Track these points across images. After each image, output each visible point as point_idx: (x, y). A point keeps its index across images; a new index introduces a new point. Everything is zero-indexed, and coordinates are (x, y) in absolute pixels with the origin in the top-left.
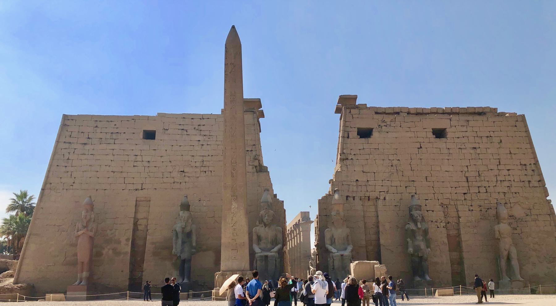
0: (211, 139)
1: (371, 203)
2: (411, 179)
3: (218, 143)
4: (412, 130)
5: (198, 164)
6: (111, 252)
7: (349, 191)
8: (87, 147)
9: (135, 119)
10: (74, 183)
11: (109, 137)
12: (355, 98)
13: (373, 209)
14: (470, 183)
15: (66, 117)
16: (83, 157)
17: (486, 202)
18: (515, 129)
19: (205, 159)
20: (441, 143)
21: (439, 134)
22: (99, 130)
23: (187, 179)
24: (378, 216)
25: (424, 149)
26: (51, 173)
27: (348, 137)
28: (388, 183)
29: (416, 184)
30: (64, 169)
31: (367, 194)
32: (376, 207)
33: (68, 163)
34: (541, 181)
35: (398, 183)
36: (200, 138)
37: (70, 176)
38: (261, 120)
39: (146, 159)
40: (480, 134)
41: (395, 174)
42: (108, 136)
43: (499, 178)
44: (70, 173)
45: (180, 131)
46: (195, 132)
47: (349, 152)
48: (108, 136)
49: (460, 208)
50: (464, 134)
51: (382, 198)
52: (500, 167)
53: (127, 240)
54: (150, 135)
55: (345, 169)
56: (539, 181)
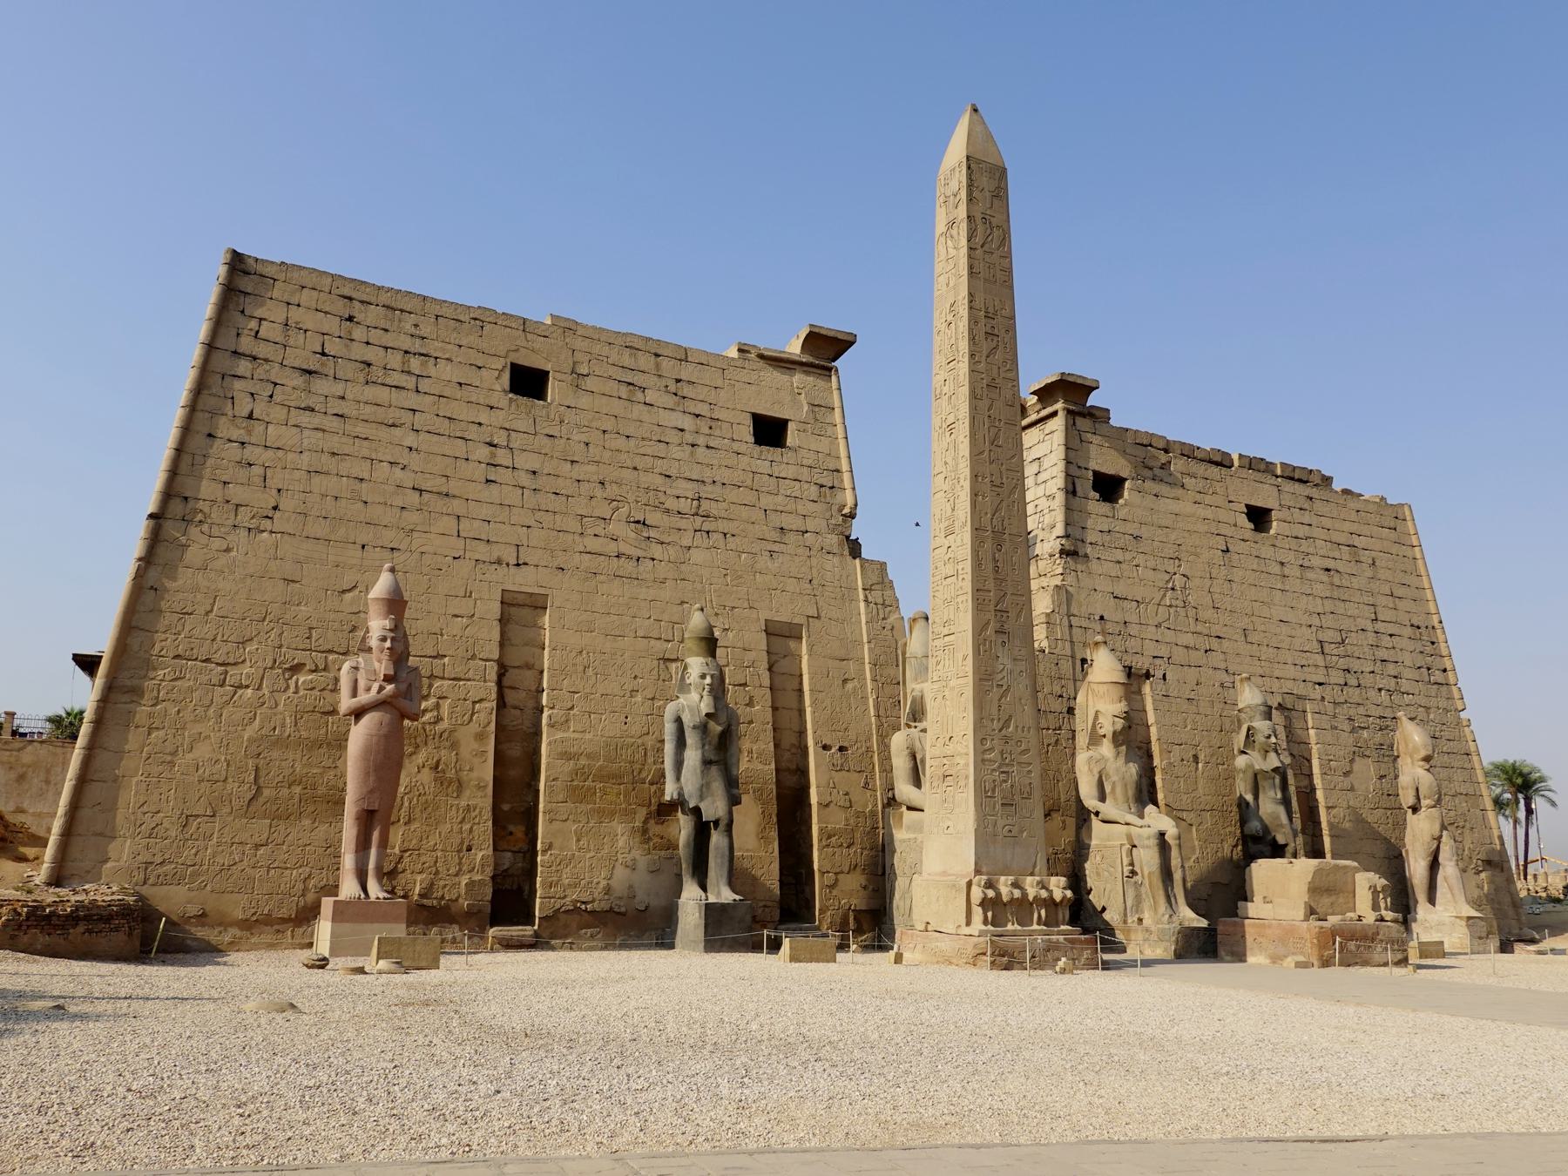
0: (717, 432)
2: (1216, 630)
3: (736, 446)
5: (684, 505)
6: (426, 776)
8: (321, 386)
9: (481, 319)
11: (397, 366)
12: (1088, 389)
15: (237, 263)
16: (305, 419)
17: (1361, 710)
18: (1393, 535)
19: (706, 491)
20: (1263, 545)
21: (1259, 517)
22: (359, 333)
26: (186, 459)
27: (1074, 493)
29: (1225, 643)
30: (234, 451)
33: (249, 432)
35: (1188, 639)
36: (687, 422)
37: (258, 480)
39: (526, 461)
42: (395, 360)
44: (257, 470)
45: (624, 391)
46: (669, 401)
48: (395, 360)
50: (1302, 531)
51: (1159, 674)
54: (528, 382)
55: (1070, 579)
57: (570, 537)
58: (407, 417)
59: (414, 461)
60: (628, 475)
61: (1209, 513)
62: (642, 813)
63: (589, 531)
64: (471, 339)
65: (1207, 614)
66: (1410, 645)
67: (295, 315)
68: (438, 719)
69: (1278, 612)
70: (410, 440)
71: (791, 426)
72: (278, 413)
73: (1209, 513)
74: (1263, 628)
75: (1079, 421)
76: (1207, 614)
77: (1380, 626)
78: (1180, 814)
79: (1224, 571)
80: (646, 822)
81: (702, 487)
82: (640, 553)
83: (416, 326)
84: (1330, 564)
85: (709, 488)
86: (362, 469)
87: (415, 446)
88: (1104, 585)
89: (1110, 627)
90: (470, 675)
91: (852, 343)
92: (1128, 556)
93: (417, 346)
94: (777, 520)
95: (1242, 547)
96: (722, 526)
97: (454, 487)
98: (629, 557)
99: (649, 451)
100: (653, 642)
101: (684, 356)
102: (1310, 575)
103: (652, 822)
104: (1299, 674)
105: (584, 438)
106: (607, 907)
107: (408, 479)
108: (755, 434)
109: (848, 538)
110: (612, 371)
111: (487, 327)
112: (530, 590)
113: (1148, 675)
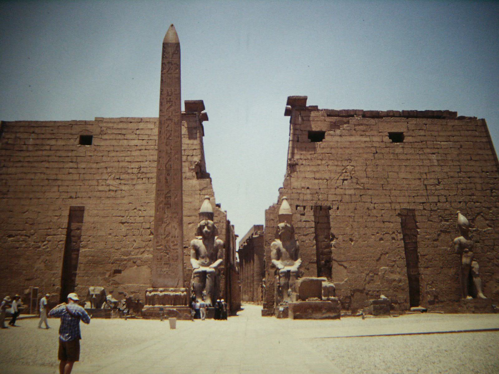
2: (366, 186)
5: (135, 171)
7: (298, 199)
9: (72, 124)
10: (8, 191)
12: (305, 99)
14: (429, 192)
19: (142, 165)
20: (398, 147)
21: (397, 137)
23: (123, 187)
27: (298, 141)
31: (319, 203)
35: (352, 192)
38: (204, 123)
51: (335, 207)
57: (94, 187)
58: (47, 158)
59: (48, 171)
60: (116, 164)
61: (368, 139)
62: (108, 274)
63: (101, 184)
64: (70, 131)
65: (364, 180)
67: (18, 135)
68: (48, 248)
70: (47, 165)
72: (11, 164)
73: (368, 139)
74: (393, 183)
78: (340, 263)
80: (110, 276)
86: (32, 176)
87: (48, 166)
90: (59, 233)
92: (324, 162)
96: (148, 175)
97: (59, 177)
98: (113, 191)
99: (124, 155)
101: (141, 120)
104: (411, 200)
105: (101, 154)
107: (45, 177)
110: (116, 131)
111: (74, 126)
112: (79, 205)
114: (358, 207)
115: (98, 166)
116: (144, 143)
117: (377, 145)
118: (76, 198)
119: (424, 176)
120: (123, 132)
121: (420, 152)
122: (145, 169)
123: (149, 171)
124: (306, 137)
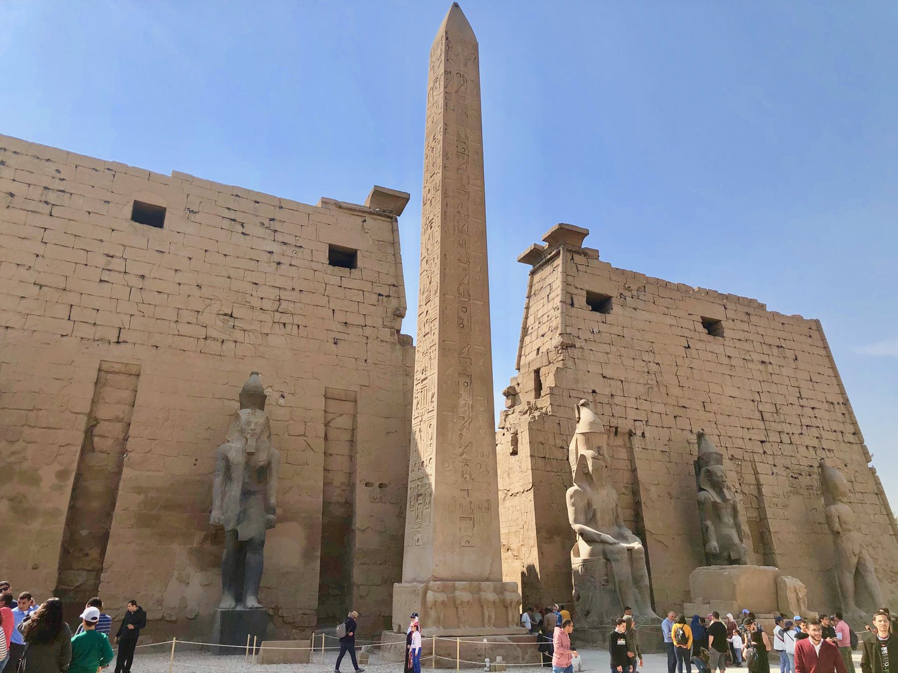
0: (300, 255)
1: (619, 441)
2: (682, 402)
4: (672, 312)
5: (267, 305)
12: (582, 234)
13: (623, 454)
19: (284, 295)
21: (712, 327)
23: (238, 335)
24: (634, 470)
25: (693, 351)
27: (572, 305)
28: (646, 406)
32: (631, 450)
34: (856, 433)
36: (274, 247)
39: (136, 269)
40: (768, 340)
41: (655, 389)
42: (36, 193)
43: (805, 421)
45: (226, 224)
47: (575, 332)
49: (761, 468)
51: (639, 433)
52: (803, 402)
53: (62, 475)
54: (149, 215)
55: (570, 364)
56: (854, 434)
62: (199, 536)
66: (827, 415)
69: (730, 391)
71: (359, 252)
73: (673, 322)
75: (576, 257)
76: (675, 391)
77: (803, 402)
79: (687, 361)
81: (282, 292)
82: (225, 337)
83: (58, 171)
84: (765, 358)
85: (288, 293)
88: (594, 369)
89: (599, 398)
91: (408, 200)
92: (614, 349)
93: (57, 185)
94: (340, 317)
95: (700, 345)
100: (227, 402)
102: (750, 365)
103: (209, 542)
104: (747, 435)
106: (160, 616)
107: (31, 276)
108: (329, 258)
109: (398, 331)
113: (631, 434)
114: (673, 438)
115: (179, 277)
116: (288, 251)
117: (687, 333)
118: (118, 342)
119: (757, 398)
120: (240, 217)
121: (748, 358)
122: (292, 305)
123: (300, 312)
124: (585, 299)
